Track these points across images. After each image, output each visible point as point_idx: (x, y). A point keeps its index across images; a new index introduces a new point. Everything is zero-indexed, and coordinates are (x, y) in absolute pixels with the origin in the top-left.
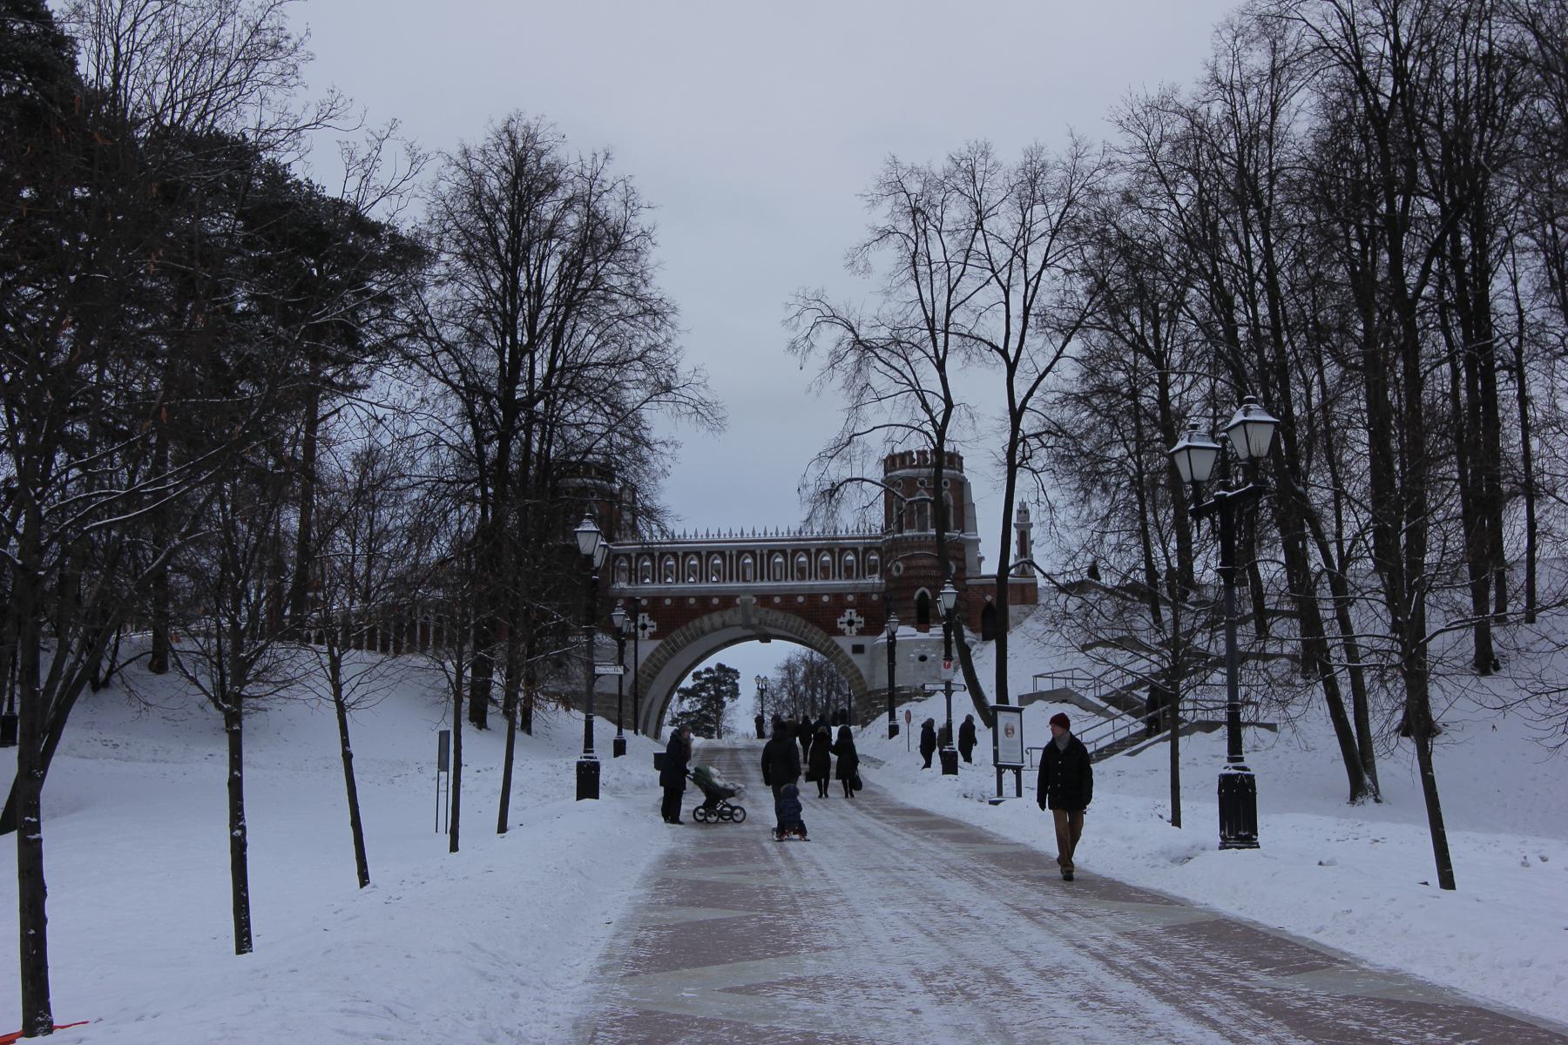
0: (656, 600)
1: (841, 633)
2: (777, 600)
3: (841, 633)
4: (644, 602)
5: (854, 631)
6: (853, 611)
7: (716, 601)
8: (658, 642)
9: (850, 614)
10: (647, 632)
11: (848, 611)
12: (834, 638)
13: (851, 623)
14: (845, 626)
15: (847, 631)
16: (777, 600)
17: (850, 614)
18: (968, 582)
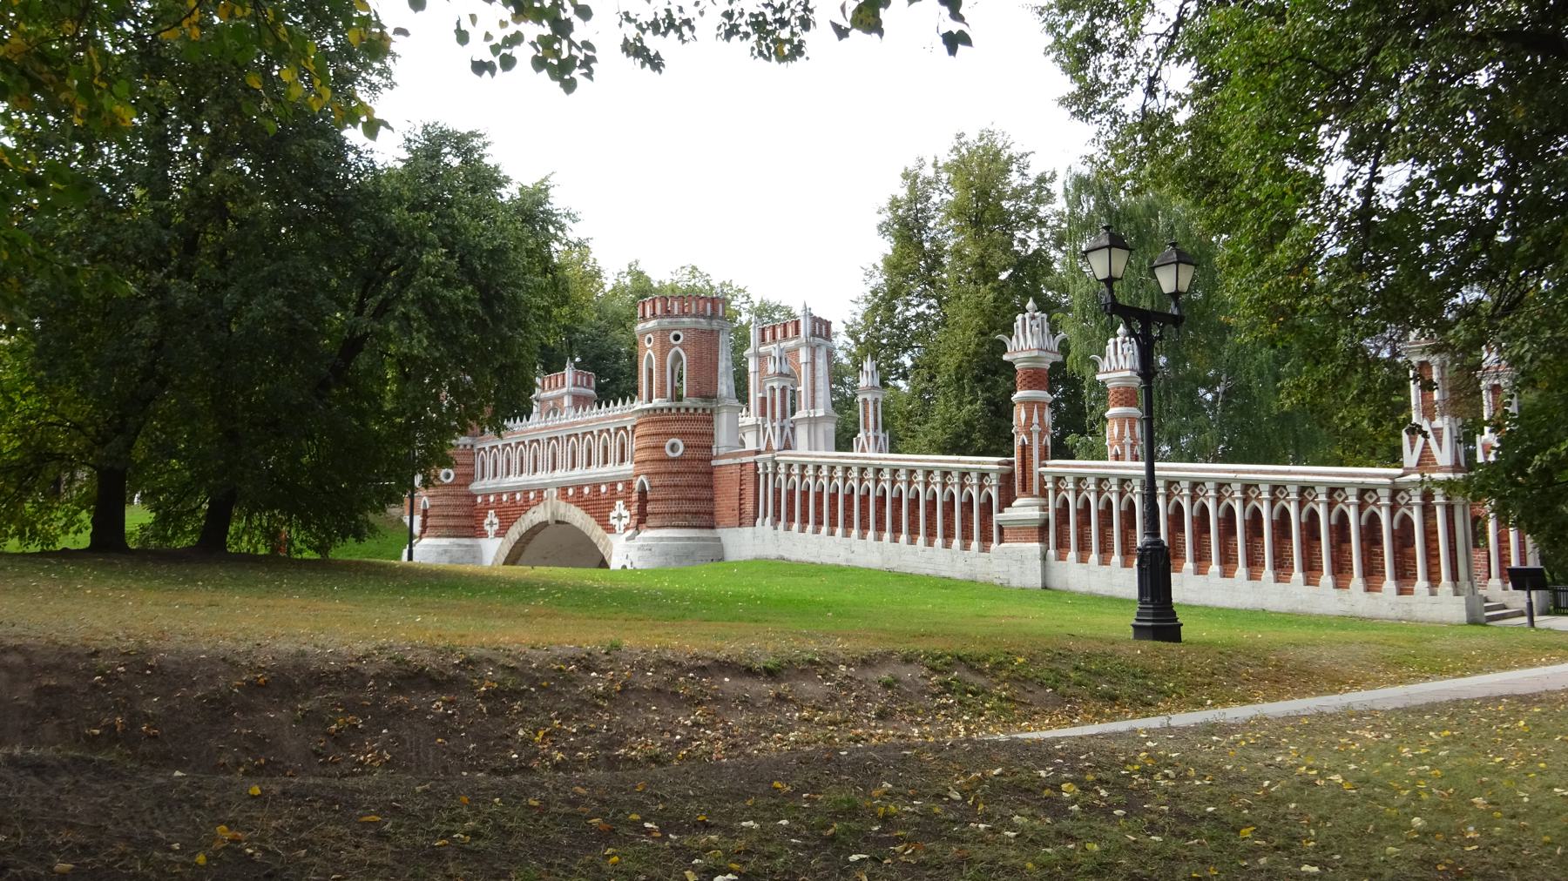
2: (571, 492)
3: (610, 529)
6: (621, 502)
7: (532, 495)
8: (501, 540)
11: (618, 503)
13: (620, 517)
16: (571, 492)
18: (714, 463)
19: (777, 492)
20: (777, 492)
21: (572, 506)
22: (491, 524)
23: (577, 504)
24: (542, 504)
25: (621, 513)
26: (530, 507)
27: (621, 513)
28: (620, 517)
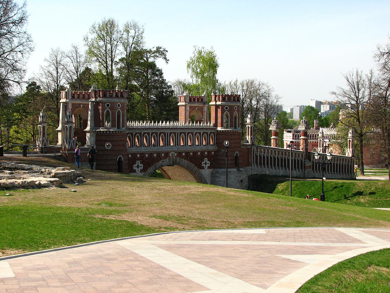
0: (142, 154)
1: (203, 168)
2: (184, 154)
3: (203, 168)
4: (138, 156)
5: (207, 167)
7: (163, 155)
9: (206, 160)
10: (139, 169)
11: (205, 159)
12: (200, 170)
13: (206, 163)
14: (204, 165)
15: (205, 167)
16: (184, 154)
17: (206, 160)
19: (256, 156)
20: (256, 156)
21: (183, 160)
22: (138, 167)
23: (186, 159)
24: (167, 159)
25: (206, 162)
26: (161, 159)
27: (206, 162)
28: (206, 163)
